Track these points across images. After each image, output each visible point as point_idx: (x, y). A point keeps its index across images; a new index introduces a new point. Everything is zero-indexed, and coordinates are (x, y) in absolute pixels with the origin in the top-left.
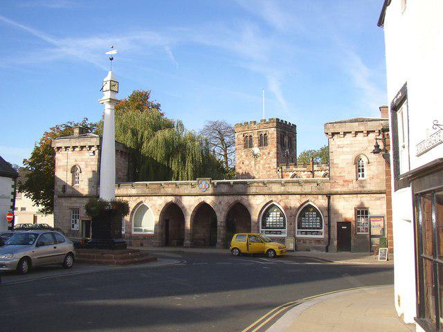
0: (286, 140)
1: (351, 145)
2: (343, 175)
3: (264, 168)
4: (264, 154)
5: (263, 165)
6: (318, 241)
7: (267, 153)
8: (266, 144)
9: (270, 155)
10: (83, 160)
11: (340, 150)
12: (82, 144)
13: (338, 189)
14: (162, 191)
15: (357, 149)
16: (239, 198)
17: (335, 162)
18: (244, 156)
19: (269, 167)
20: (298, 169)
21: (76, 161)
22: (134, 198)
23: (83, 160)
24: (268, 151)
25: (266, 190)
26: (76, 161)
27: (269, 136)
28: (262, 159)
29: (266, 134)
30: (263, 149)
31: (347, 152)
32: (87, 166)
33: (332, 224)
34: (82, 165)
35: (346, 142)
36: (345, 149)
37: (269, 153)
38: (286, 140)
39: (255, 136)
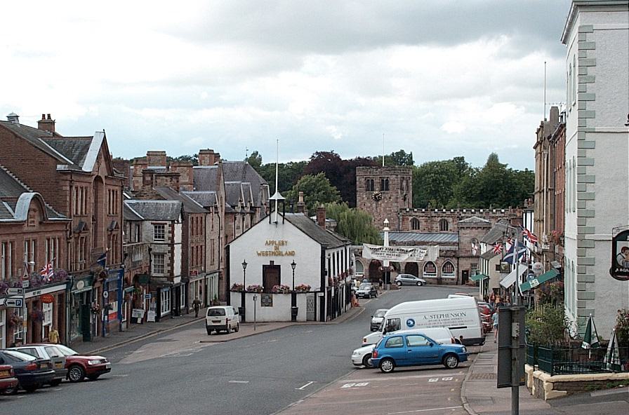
0: (404, 184)
1: (470, 233)
3: (385, 210)
4: (385, 198)
5: (384, 208)
6: (453, 279)
8: (387, 189)
13: (463, 255)
19: (391, 211)
20: (417, 214)
27: (390, 183)
28: (384, 202)
29: (387, 180)
37: (390, 198)
38: (404, 184)
39: (377, 181)
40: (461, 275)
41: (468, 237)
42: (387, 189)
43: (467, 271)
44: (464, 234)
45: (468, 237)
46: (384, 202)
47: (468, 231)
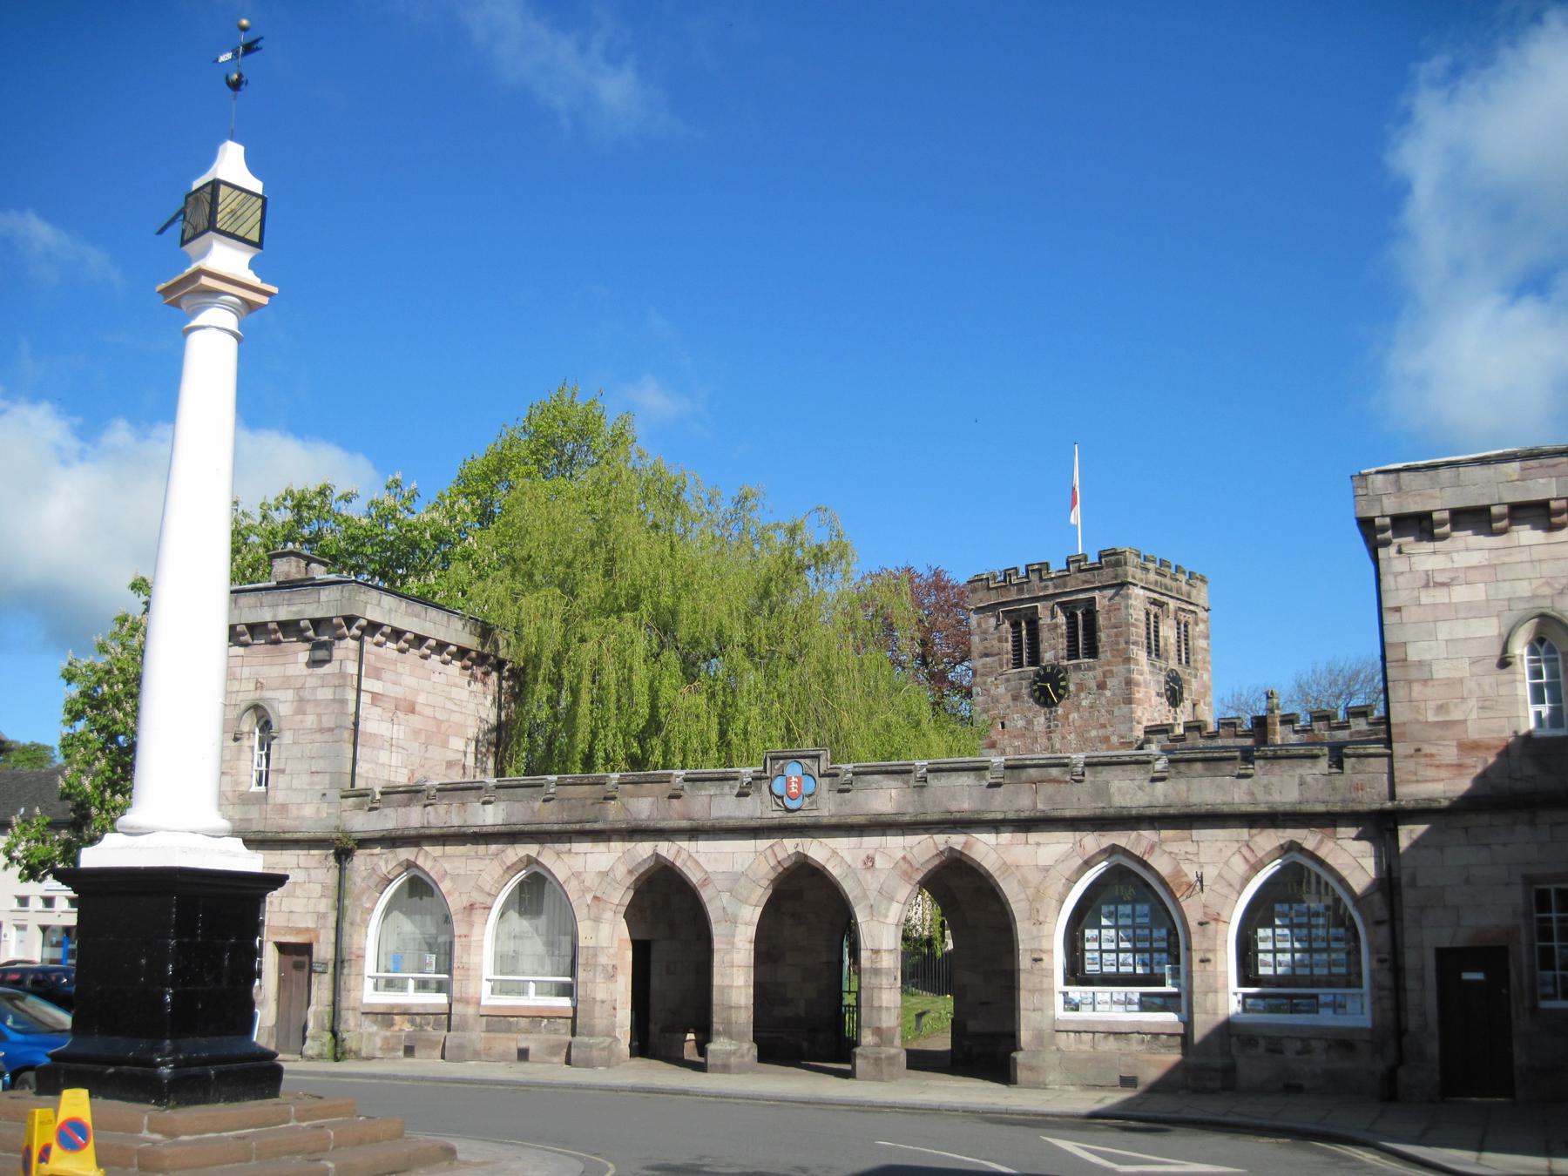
0: (1168, 632)
2: (1455, 715)
4: (1081, 687)
6: (1343, 1042)
7: (1093, 684)
9: (1108, 693)
10: (286, 684)
11: (1440, 596)
12: (284, 614)
14: (614, 814)
15: (1524, 589)
16: (957, 840)
17: (1413, 655)
18: (1008, 699)
19: (1106, 740)
21: (259, 686)
22: (493, 848)
23: (286, 684)
24: (1099, 672)
25: (1079, 801)
26: (259, 686)
27: (1101, 620)
28: (1078, 707)
30: (1077, 667)
31: (1470, 606)
32: (301, 705)
33: (1410, 960)
34: (282, 706)
35: (1462, 560)
36: (1460, 594)
37: (1102, 686)
38: (1168, 632)
40: (1424, 996)
41: (1472, 610)
42: (1092, 651)
43: (1491, 955)
44: (1429, 583)
45: (1472, 610)
46: (1078, 707)
47: (1468, 548)
